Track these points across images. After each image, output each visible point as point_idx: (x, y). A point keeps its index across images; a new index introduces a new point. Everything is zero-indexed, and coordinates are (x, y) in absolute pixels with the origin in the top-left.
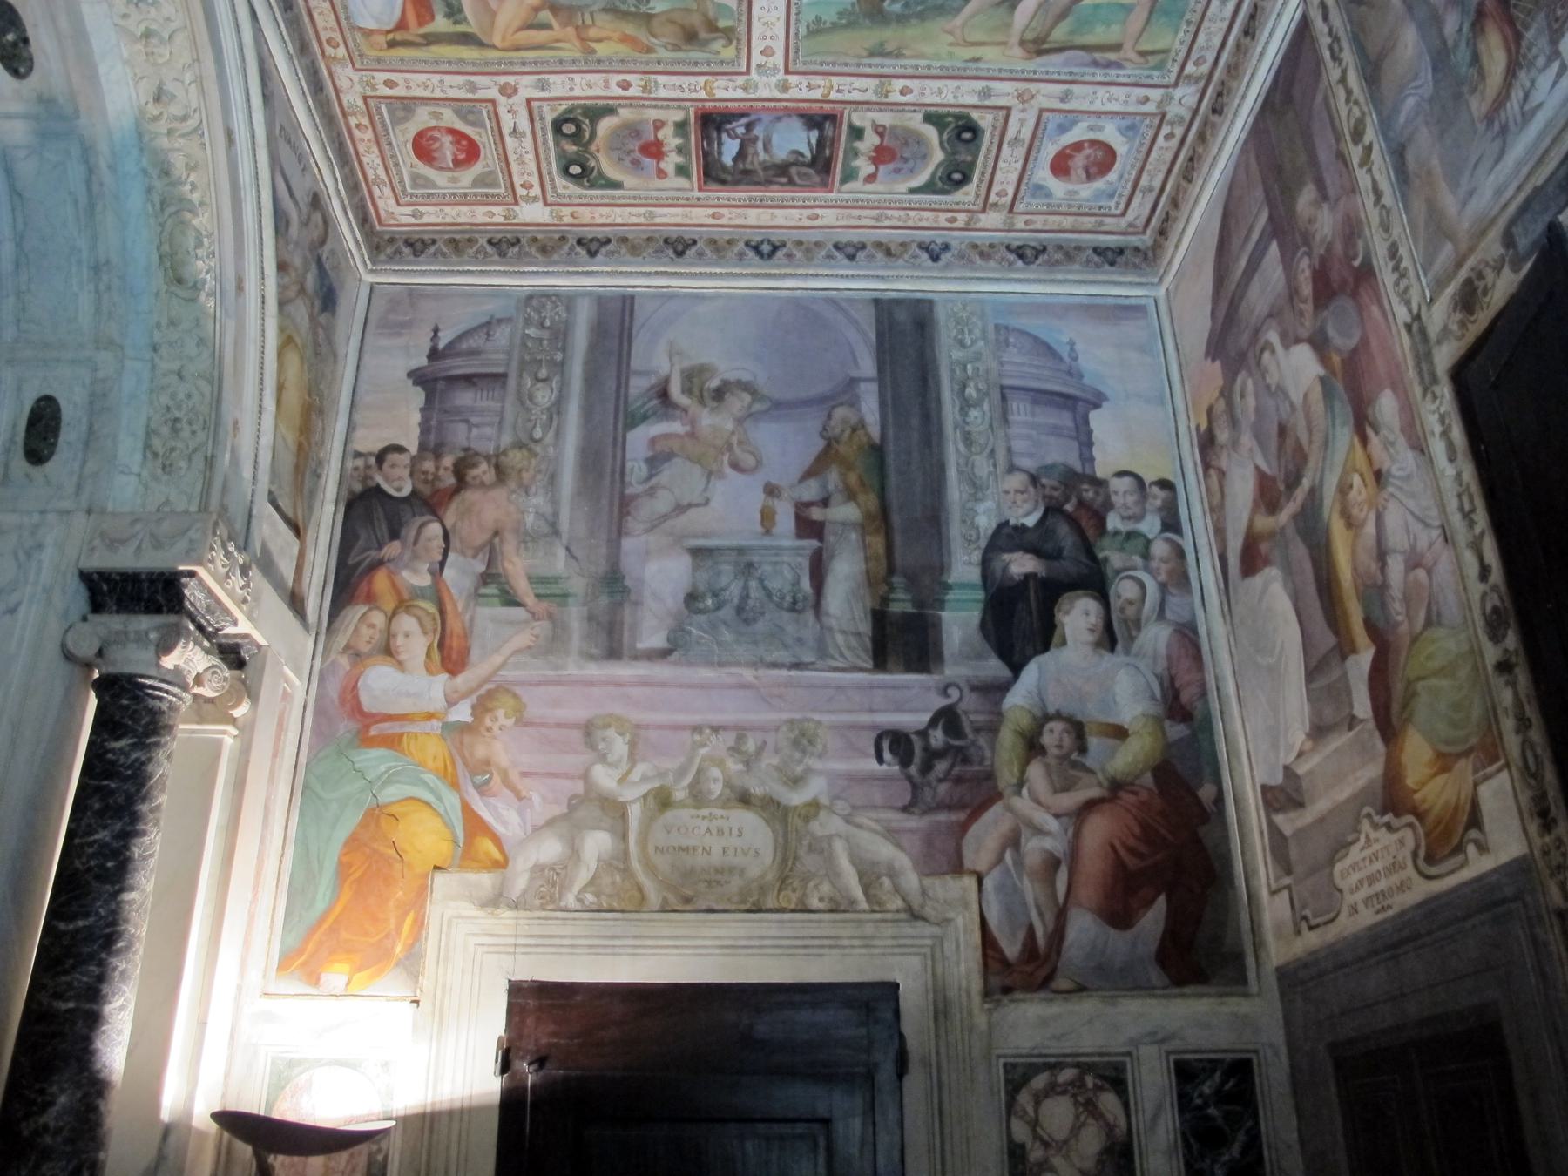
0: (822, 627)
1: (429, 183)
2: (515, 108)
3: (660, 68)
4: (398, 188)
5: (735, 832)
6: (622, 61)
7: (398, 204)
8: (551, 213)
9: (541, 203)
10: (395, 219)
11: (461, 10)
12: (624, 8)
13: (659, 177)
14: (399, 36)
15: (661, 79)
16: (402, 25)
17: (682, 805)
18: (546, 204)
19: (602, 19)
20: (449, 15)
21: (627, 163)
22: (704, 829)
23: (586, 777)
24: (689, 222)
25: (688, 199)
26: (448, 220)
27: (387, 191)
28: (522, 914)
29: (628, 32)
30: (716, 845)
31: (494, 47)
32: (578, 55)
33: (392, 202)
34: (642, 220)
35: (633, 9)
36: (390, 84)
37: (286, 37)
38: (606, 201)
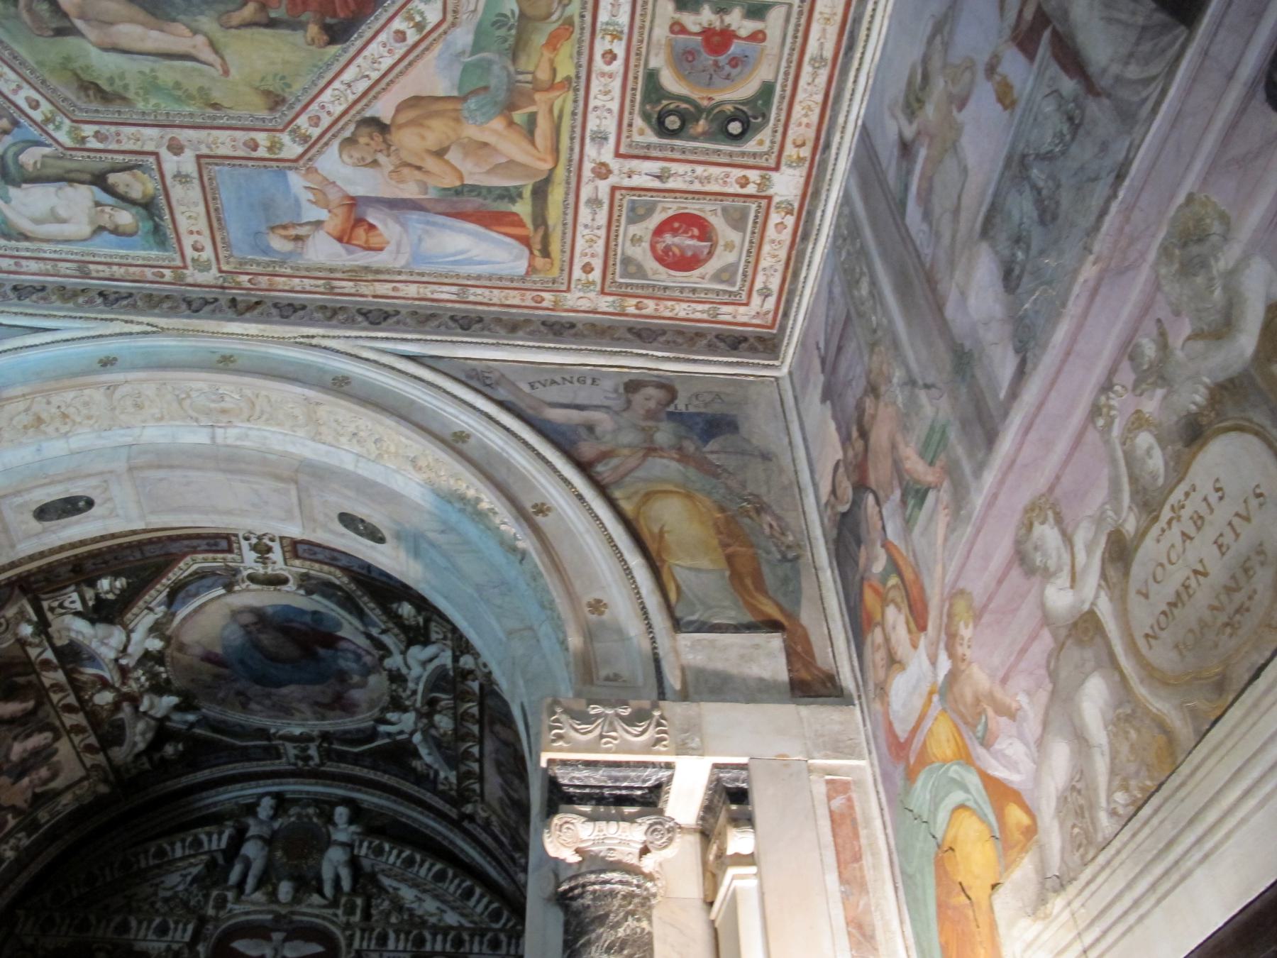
0: (1109, 96)
1: (730, 270)
2: (625, 170)
3: (588, 19)
4: (726, 298)
5: (1213, 498)
6: (579, 53)
7: (747, 304)
8: (790, 166)
9: (775, 176)
10: (767, 313)
11: (506, 189)
12: (511, 41)
13: (764, 39)
14: (537, 247)
15: (603, 17)
16: (525, 241)
17: (1142, 534)
18: (777, 168)
19: (526, 63)
20: (512, 200)
21: (734, 72)
22: (1178, 540)
23: (1046, 619)
24: (838, 18)
25: (800, 13)
26: (780, 267)
27: (725, 309)
28: (1072, 890)
29: (543, 40)
30: (1203, 548)
31: (552, 171)
32: (571, 95)
33: (742, 309)
34: (823, 75)
35: (513, 32)
36: (587, 269)
37: (479, 340)
38: (785, 106)
